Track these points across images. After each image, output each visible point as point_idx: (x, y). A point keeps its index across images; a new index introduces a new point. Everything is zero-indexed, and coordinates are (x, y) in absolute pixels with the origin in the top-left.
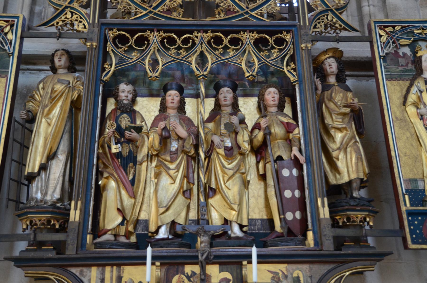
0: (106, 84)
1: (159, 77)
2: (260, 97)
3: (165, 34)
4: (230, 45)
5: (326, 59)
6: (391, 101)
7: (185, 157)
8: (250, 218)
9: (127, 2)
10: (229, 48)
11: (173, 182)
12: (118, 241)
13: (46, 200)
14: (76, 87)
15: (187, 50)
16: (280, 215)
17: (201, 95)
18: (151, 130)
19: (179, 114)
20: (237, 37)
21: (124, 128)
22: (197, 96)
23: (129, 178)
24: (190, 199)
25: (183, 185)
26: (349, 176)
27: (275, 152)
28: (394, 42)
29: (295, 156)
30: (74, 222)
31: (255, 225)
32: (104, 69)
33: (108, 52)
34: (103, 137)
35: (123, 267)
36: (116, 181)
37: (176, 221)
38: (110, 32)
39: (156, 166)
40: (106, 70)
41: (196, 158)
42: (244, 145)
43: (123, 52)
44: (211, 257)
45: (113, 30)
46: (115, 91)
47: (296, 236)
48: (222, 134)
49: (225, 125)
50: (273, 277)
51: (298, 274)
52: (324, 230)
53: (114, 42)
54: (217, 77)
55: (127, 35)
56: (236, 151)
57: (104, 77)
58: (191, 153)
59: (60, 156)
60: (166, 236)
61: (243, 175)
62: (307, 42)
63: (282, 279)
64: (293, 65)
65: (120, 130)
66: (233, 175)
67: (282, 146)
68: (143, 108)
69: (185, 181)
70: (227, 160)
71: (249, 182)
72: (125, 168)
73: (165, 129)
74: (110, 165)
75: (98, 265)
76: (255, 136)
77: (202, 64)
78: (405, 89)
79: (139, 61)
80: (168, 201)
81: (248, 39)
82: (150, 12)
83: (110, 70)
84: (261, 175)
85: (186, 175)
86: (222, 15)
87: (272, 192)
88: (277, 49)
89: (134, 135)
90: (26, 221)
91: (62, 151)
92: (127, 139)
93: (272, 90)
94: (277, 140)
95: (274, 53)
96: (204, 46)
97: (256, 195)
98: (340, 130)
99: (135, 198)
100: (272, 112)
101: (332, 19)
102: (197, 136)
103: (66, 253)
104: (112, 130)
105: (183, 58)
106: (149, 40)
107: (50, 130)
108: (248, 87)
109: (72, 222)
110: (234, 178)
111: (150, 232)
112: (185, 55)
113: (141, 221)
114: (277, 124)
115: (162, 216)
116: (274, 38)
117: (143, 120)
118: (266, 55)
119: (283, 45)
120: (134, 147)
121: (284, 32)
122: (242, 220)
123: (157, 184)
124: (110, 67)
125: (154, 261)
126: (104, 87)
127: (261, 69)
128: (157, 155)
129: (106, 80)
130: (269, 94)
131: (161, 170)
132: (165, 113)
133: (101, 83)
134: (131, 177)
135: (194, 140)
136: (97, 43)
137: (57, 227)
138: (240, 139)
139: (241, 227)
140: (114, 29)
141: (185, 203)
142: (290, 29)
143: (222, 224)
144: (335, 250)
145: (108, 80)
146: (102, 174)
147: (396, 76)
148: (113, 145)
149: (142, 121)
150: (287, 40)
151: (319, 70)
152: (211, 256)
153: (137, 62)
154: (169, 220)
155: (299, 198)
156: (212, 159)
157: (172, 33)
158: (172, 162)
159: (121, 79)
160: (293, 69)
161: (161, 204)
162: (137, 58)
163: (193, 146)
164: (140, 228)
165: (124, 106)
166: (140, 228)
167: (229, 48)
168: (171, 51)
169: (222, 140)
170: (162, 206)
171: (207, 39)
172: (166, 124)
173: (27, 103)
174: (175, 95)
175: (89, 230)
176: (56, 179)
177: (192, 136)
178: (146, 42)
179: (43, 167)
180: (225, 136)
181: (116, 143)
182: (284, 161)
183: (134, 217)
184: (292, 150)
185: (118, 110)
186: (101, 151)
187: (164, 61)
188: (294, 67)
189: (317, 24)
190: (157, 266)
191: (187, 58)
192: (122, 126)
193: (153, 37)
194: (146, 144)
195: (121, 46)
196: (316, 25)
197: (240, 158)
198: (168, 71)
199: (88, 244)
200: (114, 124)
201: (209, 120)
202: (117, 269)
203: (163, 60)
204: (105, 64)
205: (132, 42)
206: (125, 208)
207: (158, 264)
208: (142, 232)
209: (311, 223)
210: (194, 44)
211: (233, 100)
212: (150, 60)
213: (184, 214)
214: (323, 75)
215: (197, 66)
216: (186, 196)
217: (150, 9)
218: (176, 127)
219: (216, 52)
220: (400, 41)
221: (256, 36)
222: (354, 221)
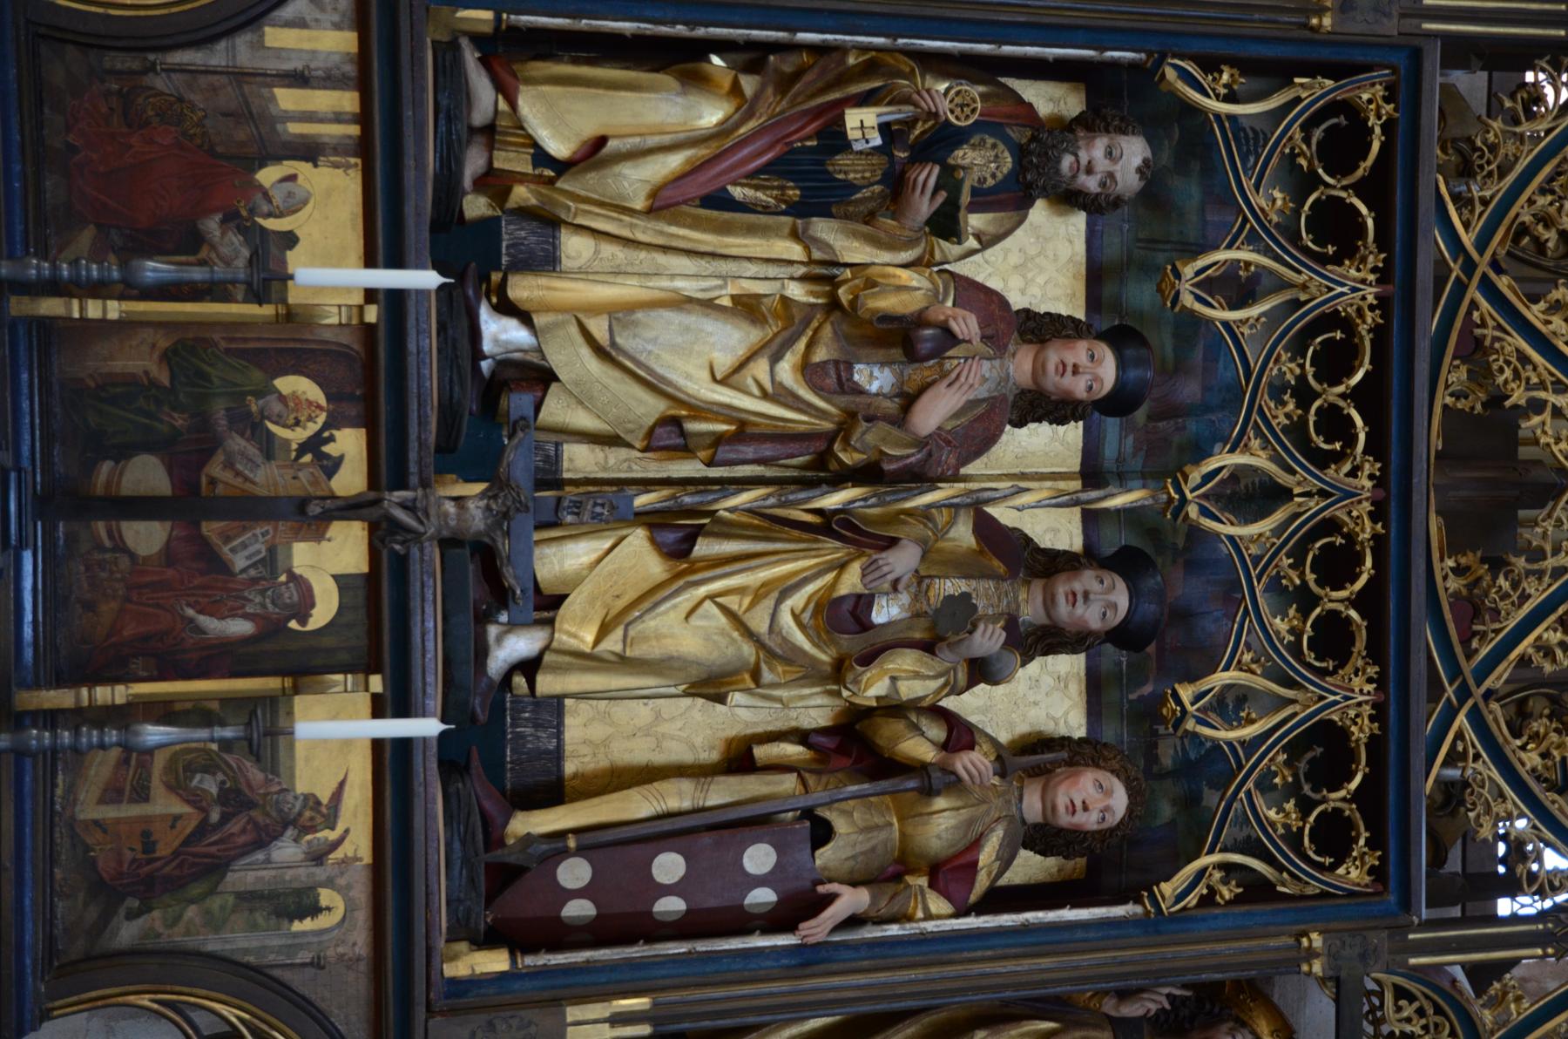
0: (1144, 77)
1: (1177, 309)
2: (1087, 750)
3: (1369, 331)
4: (1319, 616)
7: (827, 426)
8: (568, 702)
9: (1517, 159)
10: (1304, 613)
11: (719, 377)
12: (469, 142)
15: (1297, 430)
16: (577, 831)
17: (1094, 494)
18: (946, 276)
19: (1011, 398)
20: (1355, 650)
21: (951, 161)
22: (1093, 473)
23: (735, 184)
24: (644, 450)
25: (707, 420)
27: (848, 814)
29: (831, 898)
31: (537, 726)
32: (1211, 65)
33: (1290, 83)
34: (913, 70)
35: (356, 165)
36: (723, 130)
37: (554, 387)
38: (1379, 91)
39: (785, 300)
42: (880, 678)
43: (1287, 151)
44: (397, 543)
45: (1387, 100)
46: (1114, 117)
47: (489, 900)
48: (924, 586)
49: (966, 597)
50: (318, 803)
51: (329, 909)
52: (515, 1022)
54: (1174, 562)
56: (850, 643)
57: (1175, 67)
58: (845, 450)
60: (487, 347)
61: (747, 677)
62: (1332, 955)
63: (309, 842)
64: (1227, 895)
66: (748, 633)
67: (873, 842)
68: (1038, 238)
69: (724, 427)
70: (812, 606)
71: (721, 699)
73: (949, 338)
74: (793, 104)
76: (916, 728)
77: (1234, 493)
79: (1246, 220)
80: (638, 356)
82: (1469, 266)
83: (1208, 96)
84: (750, 750)
85: (749, 430)
86: (1454, 584)
87: (677, 797)
88: (1301, 824)
89: (924, 206)
92: (903, 172)
93: (1119, 801)
94: (901, 820)
95: (1280, 810)
96: (1314, 504)
97: (664, 728)
100: (1021, 799)
102: (920, 477)
104: (944, 106)
105: (1261, 412)
106: (1340, 264)
108: (1133, 697)
110: (736, 634)
111: (504, 280)
112: (1274, 423)
113: (554, 237)
114: (970, 822)
115: (574, 330)
116: (1350, 810)
117: (987, 241)
118: (1275, 774)
119: (1317, 853)
120: (871, 205)
121: (1379, 858)
122: (557, 669)
123: (708, 305)
124: (1223, 91)
125: (381, 297)
126: (1133, 66)
127: (1209, 751)
128: (834, 305)
129: (1163, 75)
130: (1101, 786)
131: (771, 321)
133: (1150, 54)
134: (737, 192)
135: (901, 464)
136: (1329, 33)
138: (906, 661)
139: (529, 667)
140: (1392, 106)
141: (630, 426)
142: (1392, 884)
143: (541, 586)
145: (1163, 87)
146: (752, 68)
148: (879, 115)
149: (984, 239)
150: (1341, 871)
151: (1208, 1006)
152: (402, 543)
154: (557, 359)
155: (650, 914)
156: (817, 541)
158: (807, 369)
159: (1166, 142)
161: (625, 326)
162: (1262, 210)
163: (873, 458)
164: (523, 234)
165: (1049, 159)
166: (523, 234)
167: (1304, 613)
168: (1292, 360)
169: (901, 587)
170: (616, 328)
171: (1346, 519)
172: (969, 342)
175: (512, 17)
177: (916, 458)
178: (1331, 249)
180: (916, 598)
181: (884, 128)
182: (809, 851)
183: (569, 208)
184: (854, 884)
185: (1029, 133)
186: (852, 60)
187: (1246, 331)
188: (1222, 897)
189: (1416, 1005)
190: (361, 308)
191: (1259, 433)
192: (960, 153)
193: (1354, 280)
194: (885, 257)
195: (1314, 141)
197: (823, 663)
198: (1201, 346)
199: (455, 12)
200: (967, 117)
201: (987, 529)
202: (348, 141)
203: (1251, 327)
205: (1334, 187)
206: (606, 172)
207: (372, 314)
208: (504, 244)
209: (545, 965)
210: (1322, 460)
211: (1074, 630)
212: (1253, 268)
213: (583, 420)
214: (1187, 1026)
215: (1224, 474)
216: (659, 431)
217: (1483, 265)
218: (957, 385)
219: (1288, 558)
221: (1361, 733)
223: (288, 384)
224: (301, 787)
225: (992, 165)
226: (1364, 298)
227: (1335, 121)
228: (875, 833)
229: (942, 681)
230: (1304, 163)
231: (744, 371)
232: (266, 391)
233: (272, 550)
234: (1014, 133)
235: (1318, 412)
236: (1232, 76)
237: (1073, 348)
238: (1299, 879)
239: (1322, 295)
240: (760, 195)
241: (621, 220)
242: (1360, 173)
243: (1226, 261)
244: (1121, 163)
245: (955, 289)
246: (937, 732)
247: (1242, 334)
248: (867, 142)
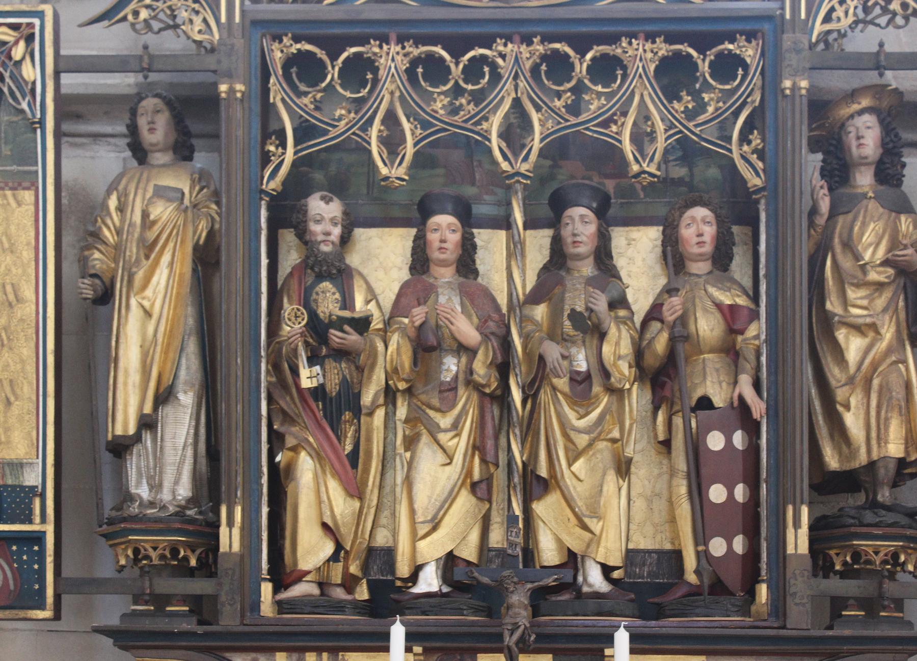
3: (417, 47)
5: (852, 116)
7: (475, 397)
8: (631, 546)
11: (448, 461)
12: (328, 596)
13: (161, 500)
14: (200, 206)
15: (478, 98)
16: (696, 544)
18: (391, 321)
19: (462, 279)
20: (612, 53)
22: (504, 223)
23: (344, 450)
24: (490, 501)
26: (869, 451)
27: (695, 386)
30: (229, 554)
32: (266, 158)
33: (274, 105)
34: (278, 343)
35: (342, 655)
38: (276, 46)
39: (407, 421)
40: (273, 158)
41: (502, 397)
44: (529, 639)
45: (281, 41)
46: (298, 218)
49: (570, 317)
53: (287, 76)
54: (561, 167)
55: (321, 54)
59: (181, 396)
61: (615, 446)
64: (759, 141)
66: (590, 445)
68: (369, 259)
69: (477, 460)
70: (576, 408)
71: (629, 461)
72: (335, 423)
77: (519, 126)
79: (354, 134)
80: (437, 507)
81: (641, 60)
83: (283, 160)
84: (660, 443)
85: (478, 444)
89: (352, 338)
90: (125, 549)
91: (186, 383)
92: (334, 350)
93: (700, 212)
94: (702, 353)
96: (522, 84)
98: (859, 329)
99: (361, 498)
102: (506, 344)
103: (221, 623)
105: (466, 121)
106: (378, 69)
109: (225, 554)
111: (399, 579)
112: (473, 113)
113: (377, 550)
114: (705, 310)
117: (372, 295)
120: (353, 368)
124: (280, 150)
125: (409, 644)
126: (270, 208)
129: (273, 190)
130: (689, 224)
131: (417, 430)
132: (424, 277)
133: (261, 199)
135: (498, 352)
137: (193, 562)
141: (477, 510)
148: (304, 368)
149: (369, 298)
150: (748, 60)
151: (832, 148)
152: (530, 636)
153: (348, 136)
155: (744, 505)
156: (540, 403)
157: (436, 46)
162: (347, 124)
163: (494, 369)
164: (375, 567)
165: (324, 259)
166: (375, 567)
169: (566, 354)
171: (531, 61)
173: (86, 253)
174: (449, 225)
176: (180, 452)
178: (369, 76)
179: (147, 424)
181: (312, 361)
183: (360, 543)
184: (736, 383)
185: (309, 271)
188: (759, 144)
190: (415, 655)
191: (478, 123)
192: (321, 315)
194: (381, 360)
195: (306, 89)
200: (302, 314)
201: (535, 298)
204: (269, 141)
205: (333, 75)
207: (418, 649)
208: (382, 578)
215: (504, 145)
216: (479, 495)
218: (452, 320)
221: (664, 49)
222: (869, 562)
225: (328, 295)
226: (398, 53)
227: (294, 76)
228: (708, 370)
229: (621, 327)
230: (319, 96)
231: (445, 447)
234: (310, 280)
235: (466, 82)
236: (271, 144)
237: (431, 242)
238: (752, 90)
239: (396, 81)
240: (349, 435)
241: (366, 514)
242: (325, 58)
243: (378, 146)
244: (324, 215)
245: (398, 316)
246: (655, 326)
247: (421, 134)
248: (318, 374)
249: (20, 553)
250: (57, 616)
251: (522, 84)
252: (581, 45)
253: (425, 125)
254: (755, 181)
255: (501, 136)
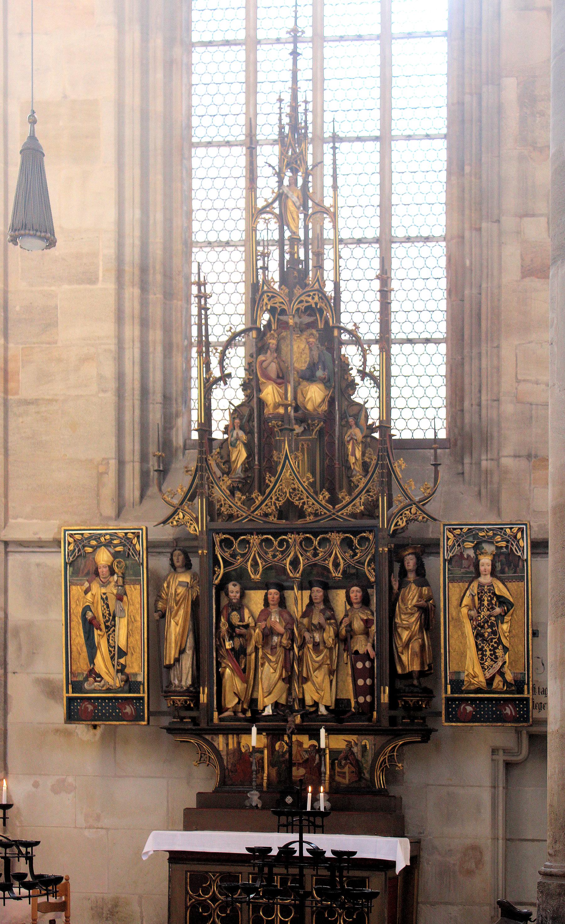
6: (450, 602)
15: (282, 552)
27: (354, 647)
28: (459, 545)
29: (367, 651)
30: (203, 703)
32: (214, 572)
36: (232, 670)
53: (221, 546)
56: (321, 647)
59: (187, 651)
65: (232, 627)
69: (284, 671)
75: (223, 734)
78: (463, 591)
89: (244, 631)
96: (297, 547)
101: (415, 512)
107: (178, 630)
126: (216, 589)
134: (243, 667)
144: (390, 725)
147: (458, 578)
160: (373, 569)
178: (247, 546)
179: (177, 660)
189: (399, 520)
191: (283, 561)
196: (398, 522)
210: (288, 547)
213: (284, 696)
220: (465, 544)
223: (277, 748)
224: (345, 747)
232: (278, 751)
233: (304, 751)
249: (136, 703)
250: (148, 723)
251: (297, 547)
252: (316, 535)
253: (266, 561)
254: (373, 579)
255: (290, 564)
